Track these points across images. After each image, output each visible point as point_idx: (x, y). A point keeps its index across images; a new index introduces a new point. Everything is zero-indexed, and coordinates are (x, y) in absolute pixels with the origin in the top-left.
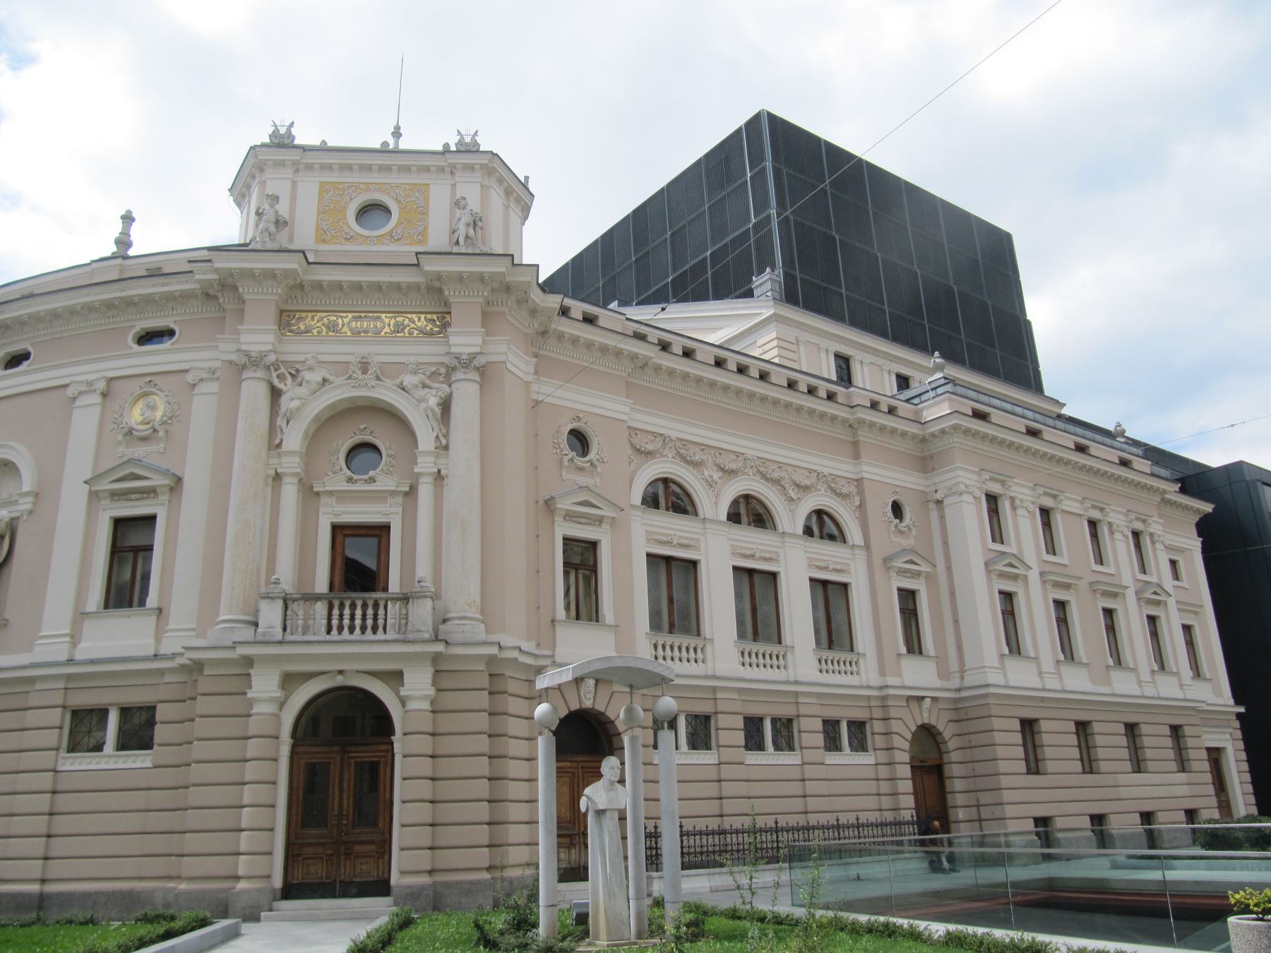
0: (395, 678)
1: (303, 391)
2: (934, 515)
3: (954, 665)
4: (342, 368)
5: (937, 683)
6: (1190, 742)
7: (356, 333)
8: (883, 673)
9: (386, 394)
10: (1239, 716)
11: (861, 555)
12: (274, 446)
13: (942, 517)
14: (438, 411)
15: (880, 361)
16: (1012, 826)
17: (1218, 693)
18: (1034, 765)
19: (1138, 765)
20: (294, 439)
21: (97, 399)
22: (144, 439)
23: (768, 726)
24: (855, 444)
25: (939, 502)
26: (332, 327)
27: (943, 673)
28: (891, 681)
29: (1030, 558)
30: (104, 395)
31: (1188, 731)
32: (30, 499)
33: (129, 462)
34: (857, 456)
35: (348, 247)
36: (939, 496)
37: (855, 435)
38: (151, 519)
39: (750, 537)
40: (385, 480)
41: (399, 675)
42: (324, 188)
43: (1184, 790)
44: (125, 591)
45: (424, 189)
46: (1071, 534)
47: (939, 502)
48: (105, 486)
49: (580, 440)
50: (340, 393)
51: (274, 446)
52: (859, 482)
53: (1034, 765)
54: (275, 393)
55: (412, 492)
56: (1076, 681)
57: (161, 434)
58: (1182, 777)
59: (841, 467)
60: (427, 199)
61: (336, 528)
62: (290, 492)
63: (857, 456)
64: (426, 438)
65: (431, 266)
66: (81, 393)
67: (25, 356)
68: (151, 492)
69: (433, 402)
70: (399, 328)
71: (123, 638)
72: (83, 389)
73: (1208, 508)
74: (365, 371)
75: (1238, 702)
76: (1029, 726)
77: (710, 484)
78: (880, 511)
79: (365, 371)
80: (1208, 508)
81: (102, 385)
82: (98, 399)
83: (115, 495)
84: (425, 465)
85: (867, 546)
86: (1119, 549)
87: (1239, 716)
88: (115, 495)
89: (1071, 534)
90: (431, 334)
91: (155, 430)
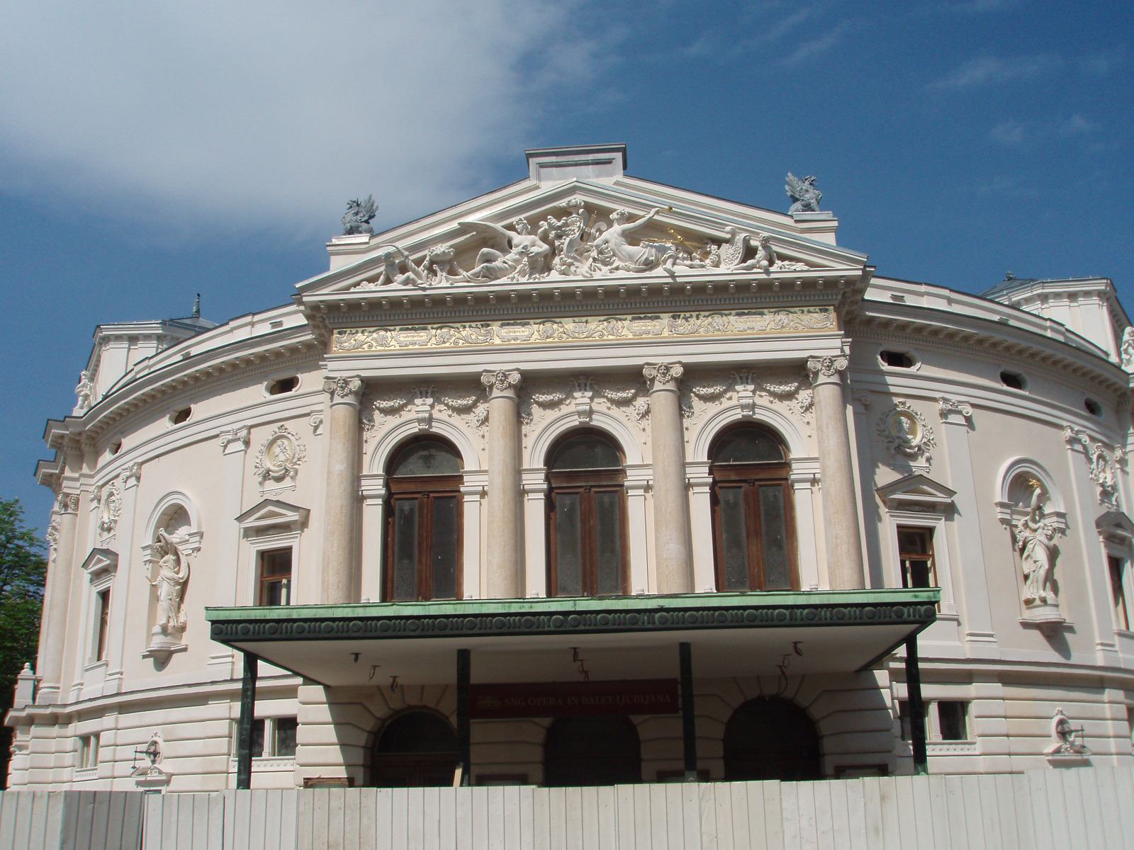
21: (240, 446)
22: (279, 479)
30: (247, 443)
32: (197, 538)
33: (267, 502)
38: (289, 549)
48: (251, 522)
57: (292, 473)
66: (229, 442)
68: (285, 527)
72: (230, 437)
81: (244, 433)
82: (243, 447)
83: (261, 531)
88: (261, 531)
91: (287, 470)
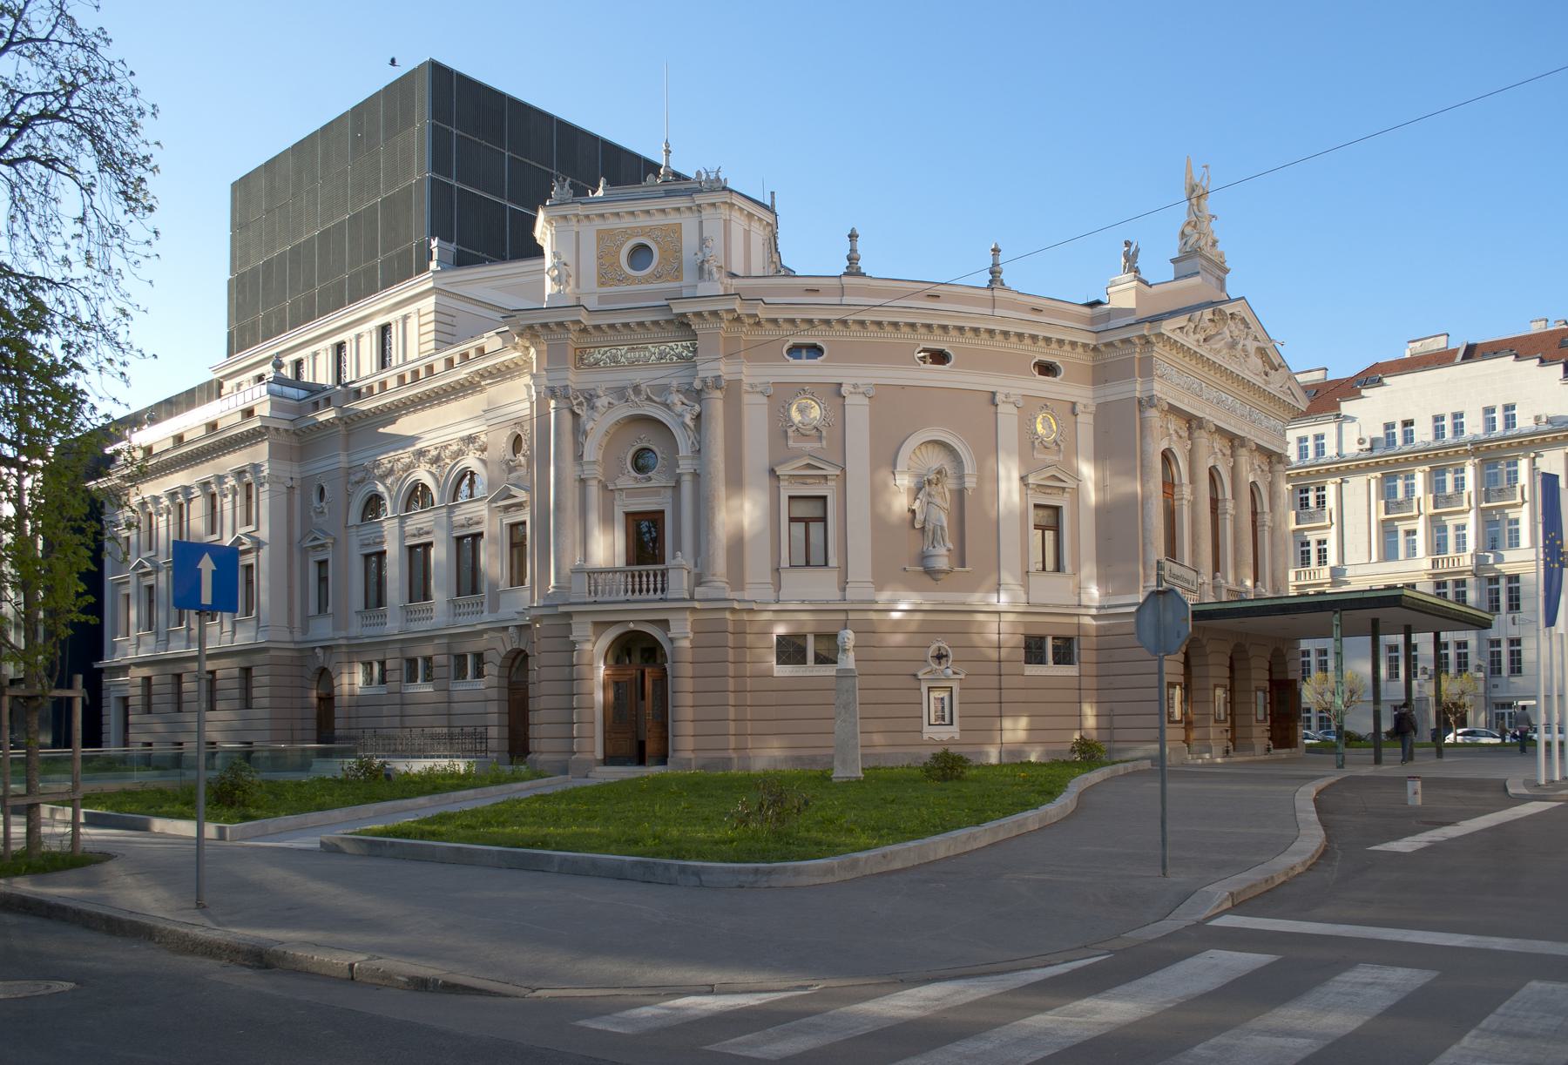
0: (664, 624)
1: (596, 416)
4: (620, 393)
12: (579, 457)
14: (691, 424)
20: (592, 450)
26: (614, 359)
35: (623, 288)
40: (657, 478)
41: (666, 621)
42: (602, 236)
50: (624, 411)
51: (579, 457)
54: (575, 415)
55: (677, 487)
60: (680, 239)
61: (627, 514)
62: (594, 491)
64: (684, 446)
65: (678, 309)
69: (688, 420)
84: (685, 467)
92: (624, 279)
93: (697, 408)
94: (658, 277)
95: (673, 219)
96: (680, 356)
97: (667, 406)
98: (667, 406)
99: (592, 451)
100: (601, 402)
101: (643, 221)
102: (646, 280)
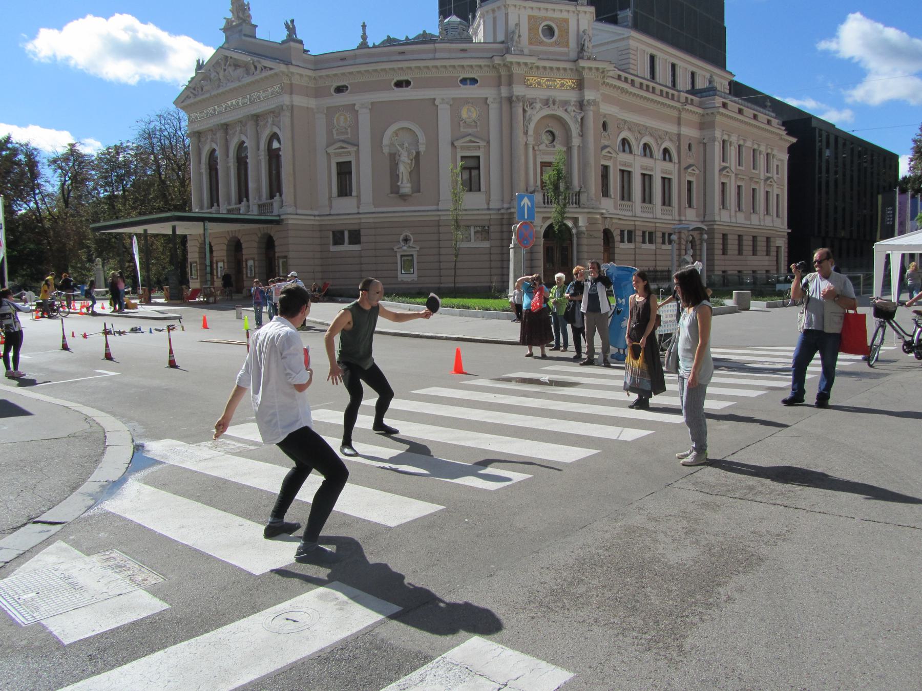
2: (702, 149)
3: (702, 212)
4: (546, 103)
5: (696, 219)
6: (772, 244)
7: (548, 86)
8: (680, 215)
9: (560, 113)
10: (788, 233)
11: (677, 166)
12: (526, 133)
13: (705, 150)
15: (666, 57)
16: (716, 273)
17: (783, 224)
18: (724, 252)
19: (754, 253)
23: (626, 232)
24: (679, 119)
25: (705, 144)
26: (539, 83)
27: (697, 216)
28: (683, 218)
29: (733, 168)
31: (772, 239)
34: (679, 124)
36: (705, 141)
37: (680, 114)
39: (648, 161)
42: (530, 18)
43: (767, 263)
44: (472, 185)
45: (566, 21)
46: (747, 156)
47: (705, 144)
49: (605, 126)
50: (546, 112)
52: (679, 135)
53: (724, 252)
56: (741, 218)
58: (767, 258)
59: (672, 129)
60: (568, 25)
63: (679, 124)
64: (575, 129)
67: (408, 83)
69: (579, 118)
70: (562, 85)
71: (473, 201)
73: (794, 140)
74: (554, 104)
75: (789, 228)
76: (725, 236)
77: (637, 139)
78: (684, 147)
79: (554, 104)
80: (794, 140)
84: (576, 142)
85: (679, 162)
86: (762, 161)
87: (788, 233)
89: (747, 156)
90: (573, 88)
92: (541, 43)
93: (582, 115)
94: (556, 44)
95: (564, 15)
96: (570, 86)
97: (566, 110)
98: (566, 110)
99: (531, 132)
100: (538, 106)
101: (550, 14)
102: (551, 45)
